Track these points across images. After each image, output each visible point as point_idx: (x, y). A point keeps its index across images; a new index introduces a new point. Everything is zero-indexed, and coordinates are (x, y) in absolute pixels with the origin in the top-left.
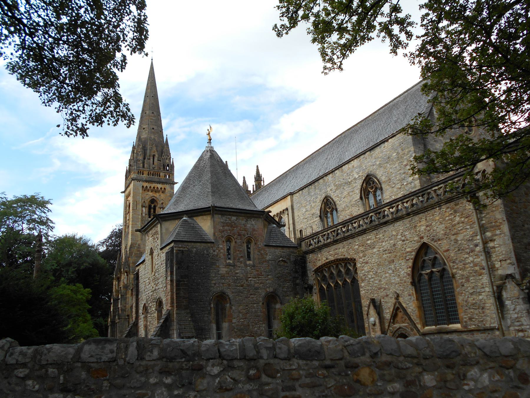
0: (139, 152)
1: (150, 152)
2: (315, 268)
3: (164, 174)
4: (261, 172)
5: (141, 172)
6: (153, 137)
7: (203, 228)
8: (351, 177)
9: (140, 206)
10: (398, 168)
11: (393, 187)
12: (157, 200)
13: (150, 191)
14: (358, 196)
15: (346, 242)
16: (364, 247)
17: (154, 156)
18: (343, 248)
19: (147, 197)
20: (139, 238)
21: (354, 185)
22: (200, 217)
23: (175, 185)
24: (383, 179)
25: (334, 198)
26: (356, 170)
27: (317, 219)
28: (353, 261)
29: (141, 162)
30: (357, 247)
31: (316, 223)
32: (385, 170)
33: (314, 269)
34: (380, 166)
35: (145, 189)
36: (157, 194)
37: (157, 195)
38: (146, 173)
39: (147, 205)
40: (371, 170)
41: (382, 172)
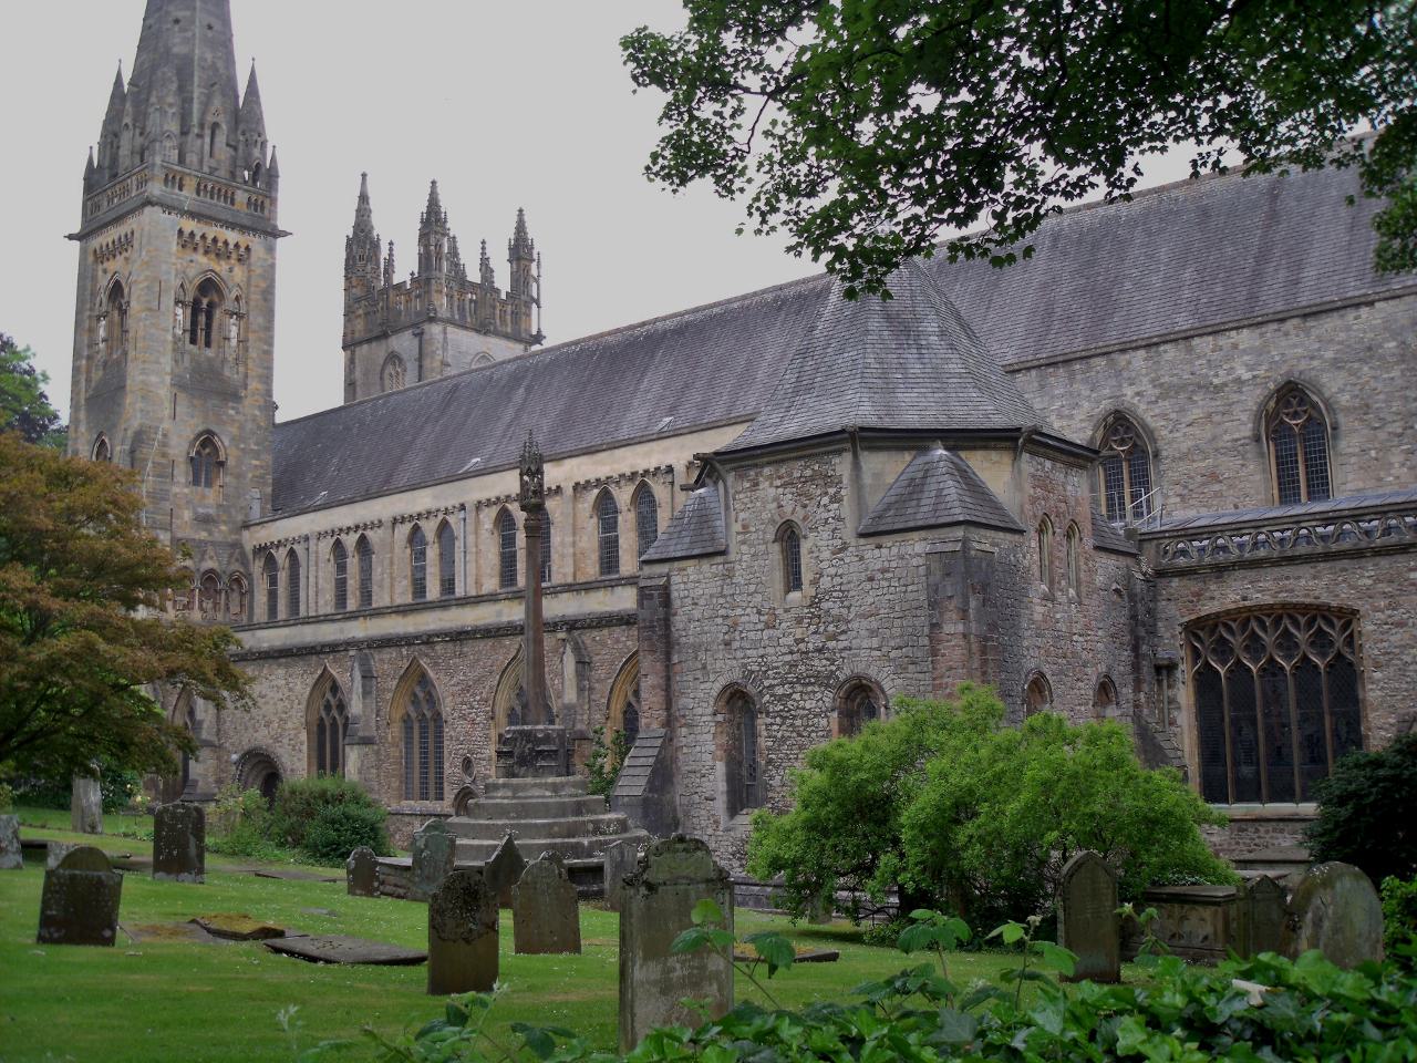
0: (171, 105)
1: (204, 113)
2: (1193, 617)
3: (246, 195)
4: (532, 232)
5: (174, 177)
6: (209, 56)
7: (989, 485)
8: (1221, 372)
9: (168, 300)
10: (1399, 382)
11: (1376, 428)
12: (222, 286)
13: (201, 250)
14: (1246, 431)
15: (1328, 565)
16: (1395, 585)
17: (215, 126)
18: (1315, 578)
19: (192, 272)
20: (167, 412)
21: (1235, 397)
22: (979, 454)
23: (279, 240)
24: (1344, 399)
26: (1246, 358)
28: (1348, 617)
29: (175, 142)
30: (1369, 582)
32: (1353, 380)
33: (1186, 619)
34: (1336, 364)
35: (187, 241)
36: (223, 263)
37: (221, 267)
38: (190, 184)
39: (189, 298)
40: (1301, 368)
41: (1341, 383)
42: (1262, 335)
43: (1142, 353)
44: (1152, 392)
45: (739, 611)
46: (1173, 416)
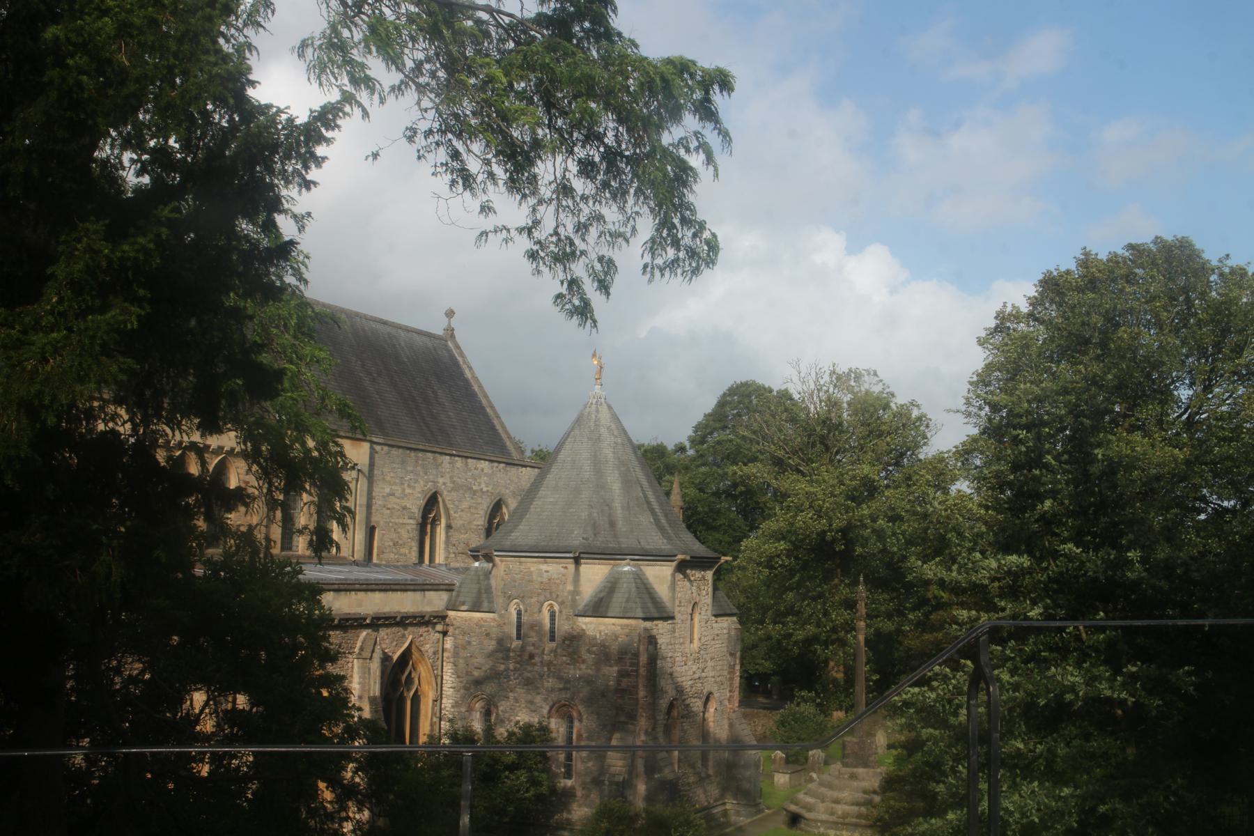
21: (480, 500)
25: (447, 502)
27: (411, 521)
31: (409, 527)
42: (492, 467)
43: (448, 457)
44: (450, 485)
45: (676, 655)
46: (456, 503)
